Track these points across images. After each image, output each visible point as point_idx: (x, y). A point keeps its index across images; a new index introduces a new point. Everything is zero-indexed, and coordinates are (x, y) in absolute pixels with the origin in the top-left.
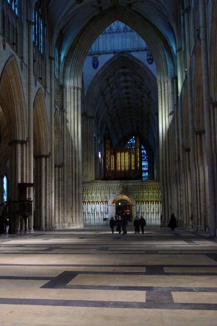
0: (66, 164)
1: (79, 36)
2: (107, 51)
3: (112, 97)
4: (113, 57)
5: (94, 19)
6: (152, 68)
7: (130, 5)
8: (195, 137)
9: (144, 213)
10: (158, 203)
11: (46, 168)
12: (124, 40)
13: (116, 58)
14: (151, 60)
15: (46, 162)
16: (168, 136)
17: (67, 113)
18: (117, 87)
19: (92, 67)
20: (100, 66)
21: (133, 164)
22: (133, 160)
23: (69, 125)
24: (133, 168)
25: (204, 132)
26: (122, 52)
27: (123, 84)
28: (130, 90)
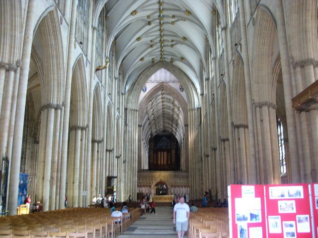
3: (152, 108)
4: (157, 86)
5: (148, 68)
6: (183, 94)
7: (172, 62)
13: (158, 86)
15: (118, 160)
20: (148, 90)
21: (169, 160)
22: (169, 157)
24: (169, 163)
26: (163, 82)
27: (161, 100)
28: (165, 103)
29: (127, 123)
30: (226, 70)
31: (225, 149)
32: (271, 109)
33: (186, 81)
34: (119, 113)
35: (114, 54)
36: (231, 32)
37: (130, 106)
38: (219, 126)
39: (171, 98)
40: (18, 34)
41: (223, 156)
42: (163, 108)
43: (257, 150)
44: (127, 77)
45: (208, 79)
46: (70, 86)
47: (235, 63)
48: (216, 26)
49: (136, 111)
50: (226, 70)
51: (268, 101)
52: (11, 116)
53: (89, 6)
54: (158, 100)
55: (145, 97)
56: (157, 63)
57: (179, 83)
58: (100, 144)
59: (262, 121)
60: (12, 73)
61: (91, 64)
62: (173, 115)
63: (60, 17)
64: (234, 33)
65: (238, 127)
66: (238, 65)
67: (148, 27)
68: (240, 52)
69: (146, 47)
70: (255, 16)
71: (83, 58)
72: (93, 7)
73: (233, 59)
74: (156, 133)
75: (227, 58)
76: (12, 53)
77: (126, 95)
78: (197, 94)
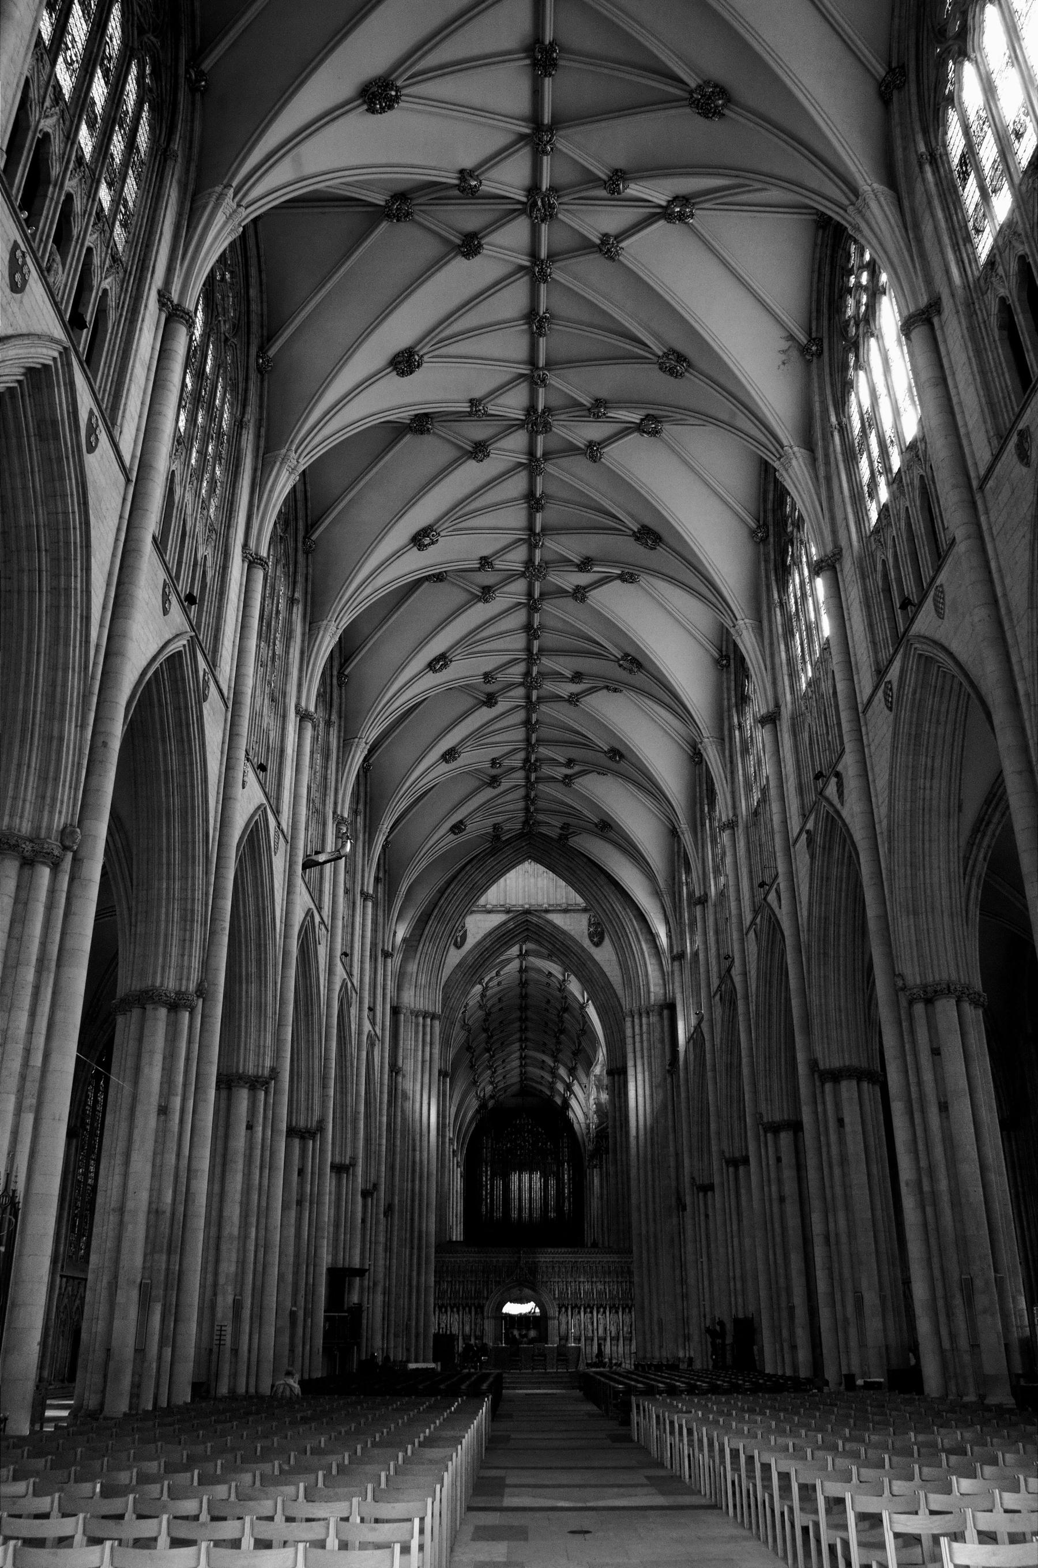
0: (397, 1208)
1: (442, 892)
4: (504, 923)
5: (477, 861)
6: (604, 955)
7: (563, 838)
8: (725, 1171)
10: (617, 1312)
11: (363, 1221)
12: (532, 880)
13: (511, 925)
14: (597, 937)
16: (652, 1145)
17: (404, 1076)
20: (471, 942)
22: (552, 1192)
23: (408, 1105)
24: (552, 1215)
25: (746, 1161)
26: (527, 912)
30: (781, 868)
31: (779, 1160)
32: (967, 1007)
33: (618, 907)
34: (373, 1023)
36: (795, 734)
37: (410, 998)
38: (753, 1074)
40: (70, 730)
41: (774, 1188)
43: (923, 1163)
44: (403, 889)
45: (703, 901)
46: (227, 925)
47: (819, 840)
48: (734, 710)
49: (433, 1017)
50: (781, 868)
51: (954, 977)
52: (30, 1032)
53: (288, 638)
55: (459, 965)
59: (936, 1052)
60: (45, 873)
61: (292, 843)
63: (201, 673)
64: (806, 735)
65: (835, 1076)
66: (828, 849)
67: (485, 714)
68: (836, 801)
69: (474, 783)
70: (894, 674)
71: (266, 820)
72: (303, 641)
73: (810, 826)
75: (785, 822)
76: (48, 800)
77: (398, 958)
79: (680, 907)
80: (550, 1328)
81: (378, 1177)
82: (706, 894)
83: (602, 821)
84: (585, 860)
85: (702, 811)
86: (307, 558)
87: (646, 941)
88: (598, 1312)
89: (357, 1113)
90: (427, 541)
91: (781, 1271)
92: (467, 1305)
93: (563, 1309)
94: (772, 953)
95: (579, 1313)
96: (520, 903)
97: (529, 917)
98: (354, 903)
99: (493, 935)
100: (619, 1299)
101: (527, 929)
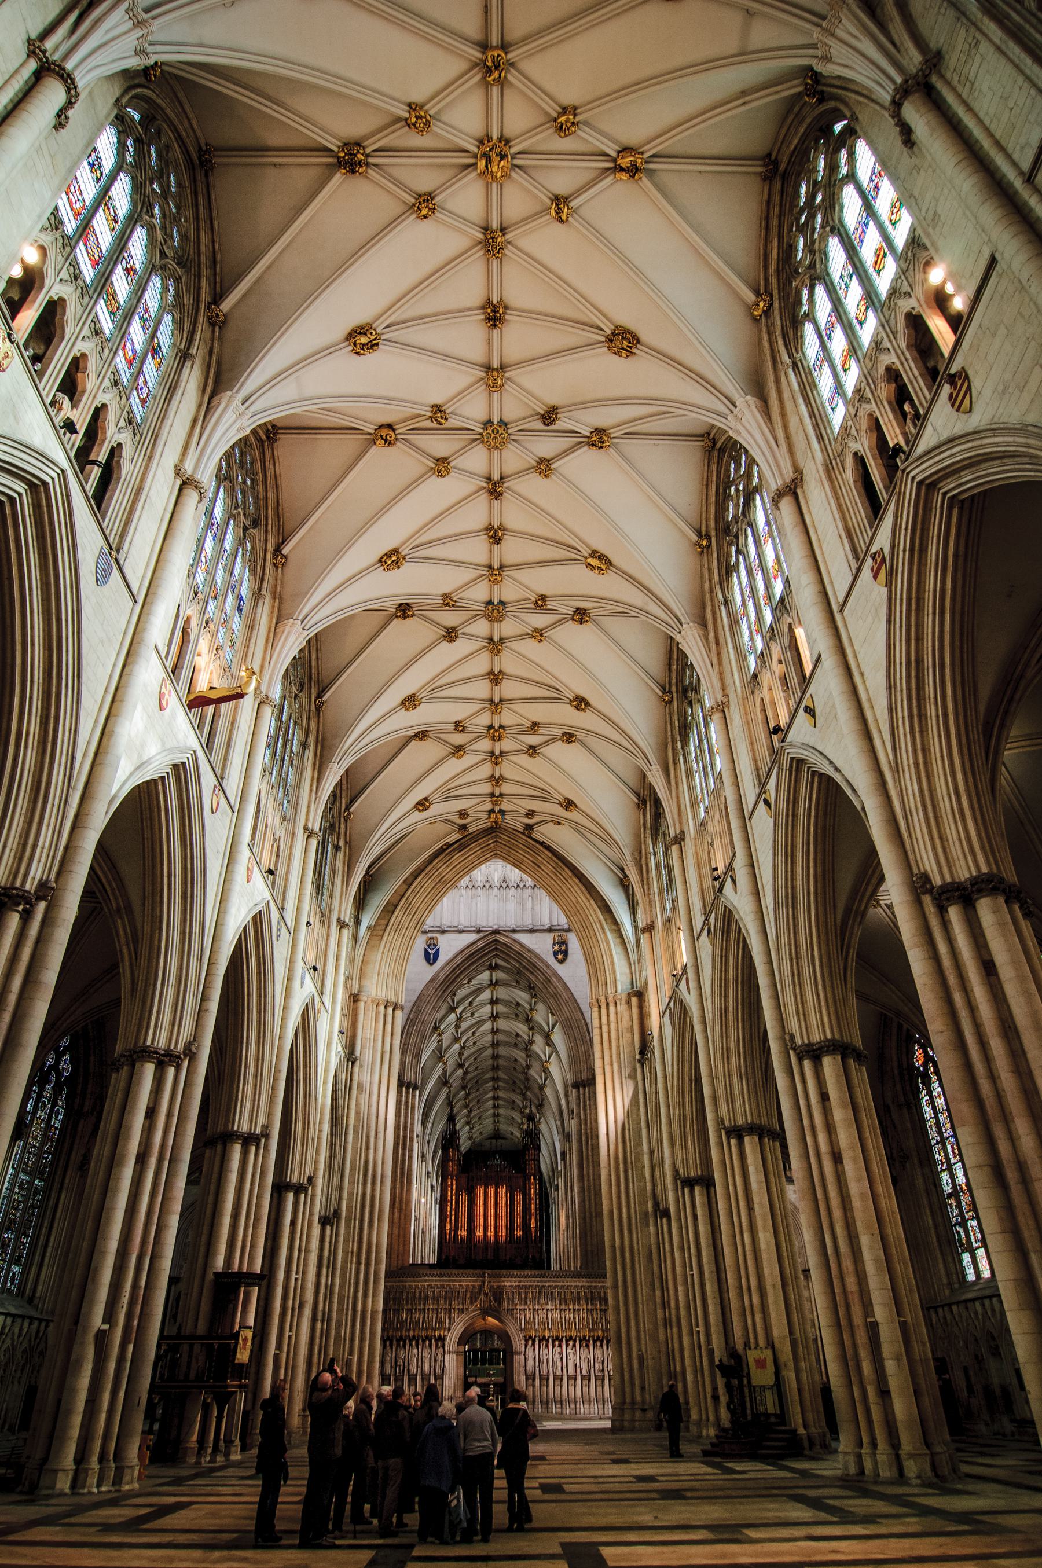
2: (461, 927)
3: (456, 1040)
4: (475, 943)
7: (529, 828)
9: (548, 1379)
10: (587, 1346)
11: (293, 1223)
13: (481, 944)
15: (296, 1203)
17: (361, 1066)
18: (472, 1015)
19: (424, 962)
21: (518, 1220)
22: (518, 1209)
23: (364, 1099)
24: (518, 1233)
26: (496, 932)
27: (489, 1007)
28: (502, 1024)
29: (358, 1053)
35: (311, 741)
39: (522, 996)
41: (822, 1137)
42: (495, 1045)
48: (718, 587)
54: (482, 1005)
55: (432, 980)
56: (476, 837)
57: (552, 935)
58: (171, 1071)
62: (528, 1067)
74: (469, 1142)
78: (623, 943)
79: (648, 879)
80: (515, 1365)
81: (316, 1170)
82: (683, 832)
83: (567, 799)
84: (550, 855)
85: (674, 749)
86: (213, 332)
87: (611, 931)
88: (567, 1346)
89: (277, 1071)
90: (363, 340)
91: (848, 1264)
92: (427, 1337)
93: (530, 1342)
94: (795, 816)
95: (547, 1346)
96: (491, 924)
97: (499, 937)
98: (293, 834)
99: (464, 953)
100: (590, 1331)
101: (496, 949)
